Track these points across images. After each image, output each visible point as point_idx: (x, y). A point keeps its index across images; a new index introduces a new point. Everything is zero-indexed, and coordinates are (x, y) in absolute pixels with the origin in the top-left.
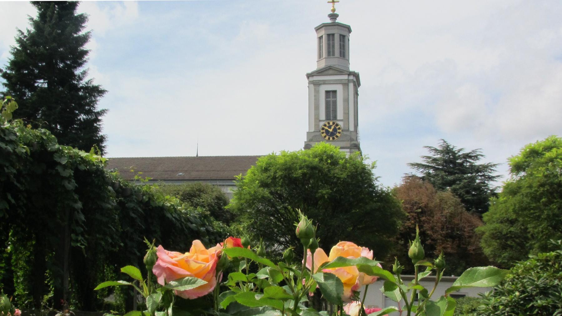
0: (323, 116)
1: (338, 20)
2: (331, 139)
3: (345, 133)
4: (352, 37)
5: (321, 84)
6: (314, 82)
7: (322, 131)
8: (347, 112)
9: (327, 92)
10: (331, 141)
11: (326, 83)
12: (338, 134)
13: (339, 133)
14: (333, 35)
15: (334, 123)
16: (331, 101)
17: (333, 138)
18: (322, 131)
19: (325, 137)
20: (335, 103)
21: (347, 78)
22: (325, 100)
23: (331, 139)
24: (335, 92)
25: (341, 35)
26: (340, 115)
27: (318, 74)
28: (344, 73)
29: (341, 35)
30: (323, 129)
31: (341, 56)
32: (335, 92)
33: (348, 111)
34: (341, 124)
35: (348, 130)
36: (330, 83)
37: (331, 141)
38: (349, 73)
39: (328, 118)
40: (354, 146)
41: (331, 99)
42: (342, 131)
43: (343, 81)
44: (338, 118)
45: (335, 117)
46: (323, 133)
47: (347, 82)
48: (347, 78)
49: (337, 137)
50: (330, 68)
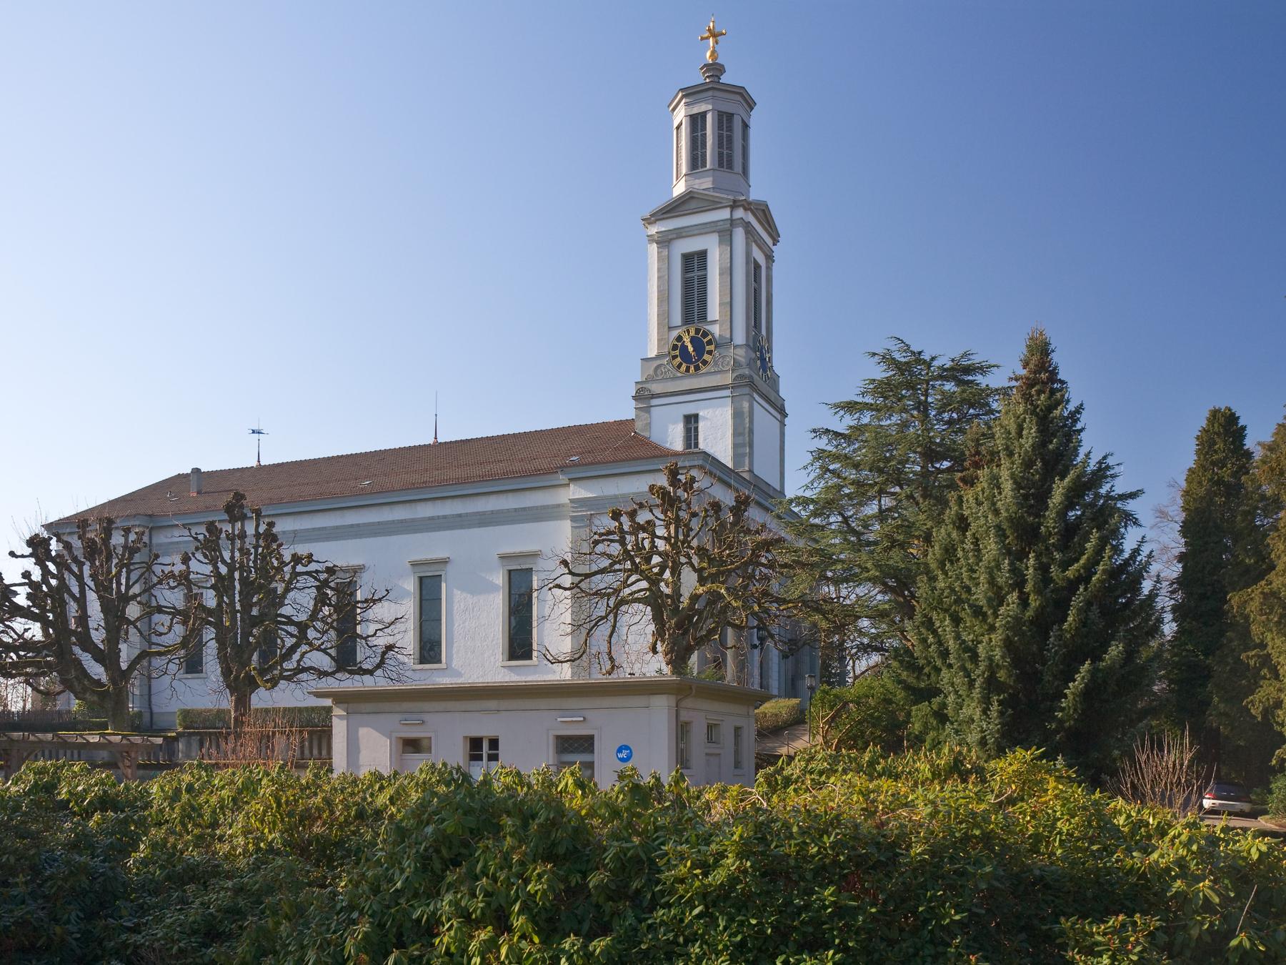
0: (677, 319)
2: (692, 368)
4: (755, 119)
5: (671, 239)
7: (673, 353)
9: (688, 259)
11: (684, 234)
13: (710, 353)
15: (697, 331)
17: (697, 368)
19: (679, 366)
20: (703, 281)
21: (729, 217)
23: (692, 368)
26: (714, 311)
27: (665, 216)
31: (721, 164)
32: (703, 255)
34: (716, 330)
36: (691, 233)
38: (731, 203)
39: (687, 319)
41: (696, 274)
42: (715, 347)
43: (722, 223)
45: (703, 317)
48: (729, 217)
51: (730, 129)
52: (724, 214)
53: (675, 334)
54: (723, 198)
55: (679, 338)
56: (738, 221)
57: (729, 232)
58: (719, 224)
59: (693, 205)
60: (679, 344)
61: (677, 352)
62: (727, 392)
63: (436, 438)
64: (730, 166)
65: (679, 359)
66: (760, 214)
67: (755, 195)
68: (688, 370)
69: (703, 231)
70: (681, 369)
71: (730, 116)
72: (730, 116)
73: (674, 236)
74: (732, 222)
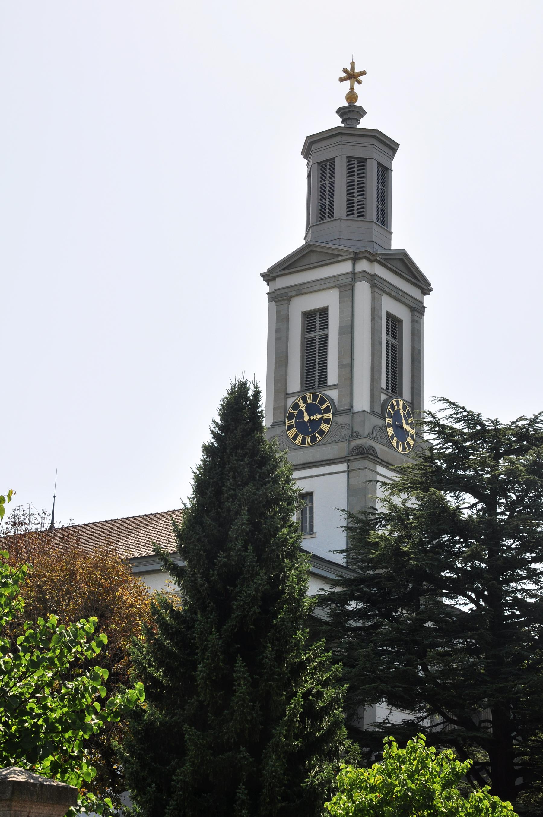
1: (364, 124)
2: (308, 440)
3: (340, 419)
6: (277, 293)
7: (288, 423)
8: (349, 361)
10: (308, 447)
11: (304, 291)
12: (324, 427)
13: (327, 421)
14: (331, 161)
15: (315, 397)
16: (317, 337)
17: (314, 439)
18: (288, 423)
19: (295, 437)
22: (303, 338)
23: (308, 440)
24: (324, 312)
25: (350, 160)
27: (284, 272)
28: (340, 259)
29: (350, 160)
30: (291, 417)
31: (350, 213)
32: (324, 312)
33: (352, 359)
35: (349, 410)
36: (309, 290)
37: (308, 447)
38: (352, 256)
40: (358, 454)
42: (333, 414)
43: (342, 277)
44: (330, 382)
46: (290, 428)
47: (350, 280)
49: (322, 432)
50: (312, 251)
51: (362, 174)
52: (346, 267)
53: (291, 401)
54: (343, 251)
55: (296, 406)
56: (361, 275)
57: (350, 287)
58: (340, 278)
59: (314, 258)
60: (295, 412)
61: (293, 422)
62: (343, 467)
63: (52, 523)
64: (362, 213)
65: (294, 430)
66: (399, 265)
67: (396, 244)
68: (304, 441)
69: (381, 281)
70: (297, 441)
71: (362, 161)
72: (362, 161)
73: (294, 293)
74: (354, 276)
